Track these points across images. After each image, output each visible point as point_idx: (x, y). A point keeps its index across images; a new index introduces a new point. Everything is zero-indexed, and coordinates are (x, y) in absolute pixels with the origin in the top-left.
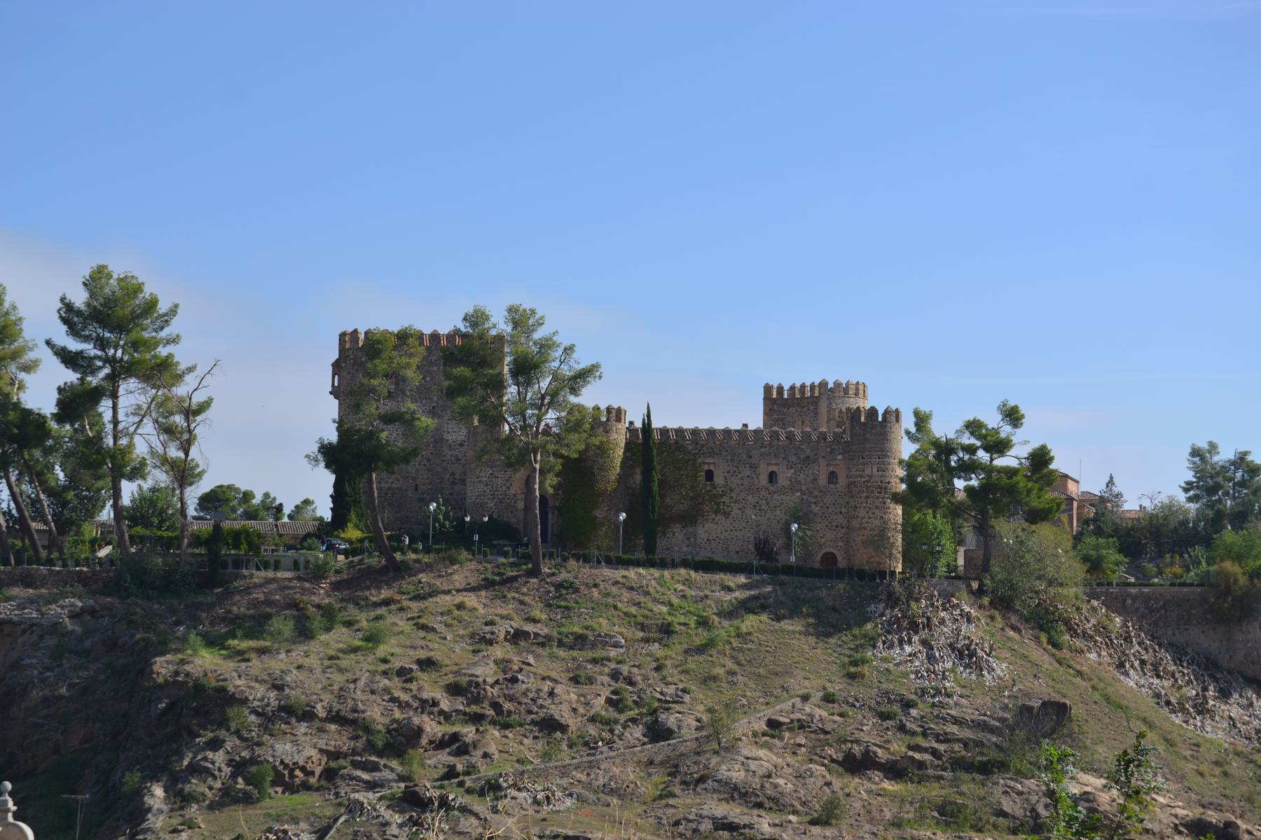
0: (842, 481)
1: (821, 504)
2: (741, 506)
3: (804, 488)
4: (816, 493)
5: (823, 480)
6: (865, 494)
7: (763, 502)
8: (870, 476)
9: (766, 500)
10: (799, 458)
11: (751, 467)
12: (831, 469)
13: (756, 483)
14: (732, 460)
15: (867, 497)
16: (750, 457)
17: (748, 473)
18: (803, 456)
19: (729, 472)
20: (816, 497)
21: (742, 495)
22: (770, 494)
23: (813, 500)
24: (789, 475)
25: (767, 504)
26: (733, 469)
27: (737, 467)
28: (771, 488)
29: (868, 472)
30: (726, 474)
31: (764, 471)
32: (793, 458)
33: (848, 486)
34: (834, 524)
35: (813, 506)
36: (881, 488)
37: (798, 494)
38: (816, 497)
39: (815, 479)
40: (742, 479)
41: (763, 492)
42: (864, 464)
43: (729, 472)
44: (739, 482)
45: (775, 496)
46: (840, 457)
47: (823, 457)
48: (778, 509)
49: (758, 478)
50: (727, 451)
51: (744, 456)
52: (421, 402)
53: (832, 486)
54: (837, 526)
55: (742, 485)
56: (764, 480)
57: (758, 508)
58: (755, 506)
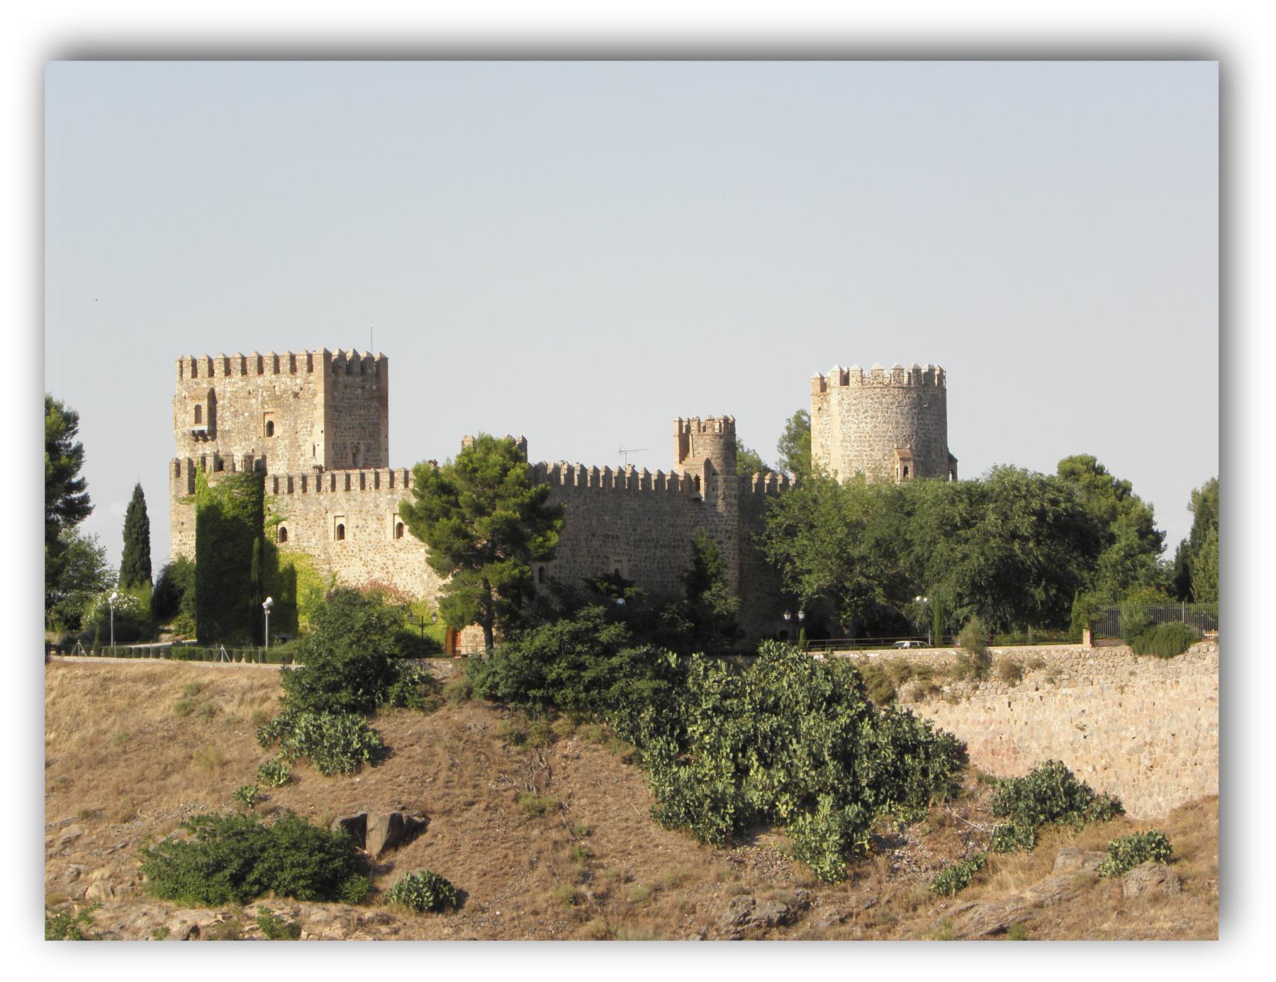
9: (393, 559)
11: (378, 519)
13: (383, 539)
17: (375, 526)
19: (357, 527)
21: (371, 555)
22: (396, 552)
25: (394, 564)
26: (361, 522)
27: (365, 520)
28: (397, 545)
30: (355, 530)
40: (370, 534)
41: (390, 550)
43: (357, 527)
45: (402, 554)
48: (404, 570)
49: (385, 533)
50: (355, 500)
52: (241, 445)
55: (370, 542)
57: (385, 571)
58: (382, 568)
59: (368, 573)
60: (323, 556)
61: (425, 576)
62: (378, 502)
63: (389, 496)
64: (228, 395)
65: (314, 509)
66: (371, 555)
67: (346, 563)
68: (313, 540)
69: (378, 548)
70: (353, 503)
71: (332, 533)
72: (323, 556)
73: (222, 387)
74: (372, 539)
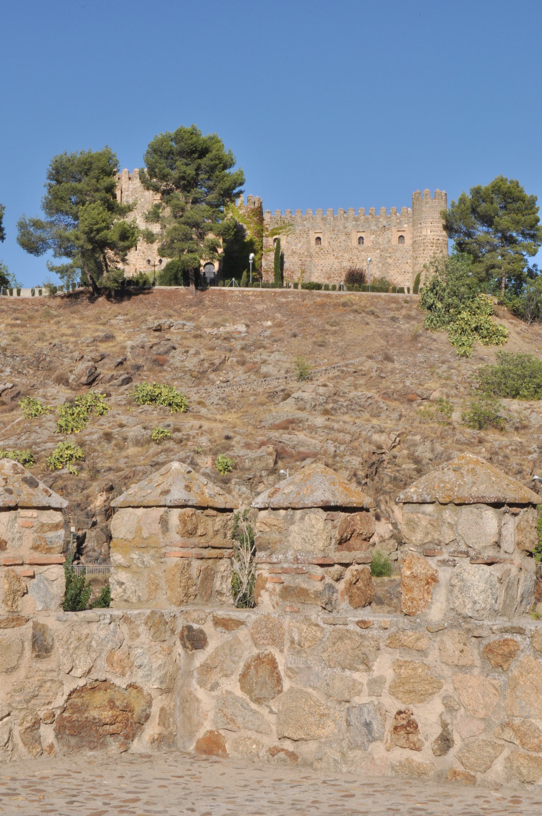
0: (408, 241)
1: (394, 257)
2: (340, 260)
3: (382, 247)
4: (390, 250)
5: (395, 240)
6: (422, 248)
7: (355, 257)
8: (426, 236)
10: (378, 227)
12: (400, 234)
13: (350, 245)
14: (334, 230)
15: (424, 250)
16: (345, 228)
17: (344, 238)
18: (381, 226)
19: (331, 238)
20: (390, 253)
21: (341, 253)
23: (389, 255)
24: (372, 239)
26: (334, 236)
28: (360, 248)
29: (424, 233)
30: (329, 240)
31: (355, 237)
32: (373, 227)
33: (412, 245)
34: (403, 271)
35: (388, 259)
36: (433, 243)
37: (378, 251)
38: (390, 253)
39: (389, 241)
41: (355, 251)
42: (421, 228)
43: (331, 238)
44: (339, 245)
45: (363, 253)
46: (406, 226)
47: (394, 226)
51: (341, 227)
53: (401, 245)
54: (405, 272)
56: (355, 242)
58: (349, 260)
59: (339, 262)
60: (306, 253)
61: (380, 265)
62: (346, 225)
63: (354, 223)
64: (131, 189)
65: (300, 228)
66: (341, 253)
67: (323, 257)
68: (299, 245)
69: (347, 249)
70: (328, 226)
71: (313, 242)
72: (306, 253)
73: (127, 185)
74: (342, 245)
